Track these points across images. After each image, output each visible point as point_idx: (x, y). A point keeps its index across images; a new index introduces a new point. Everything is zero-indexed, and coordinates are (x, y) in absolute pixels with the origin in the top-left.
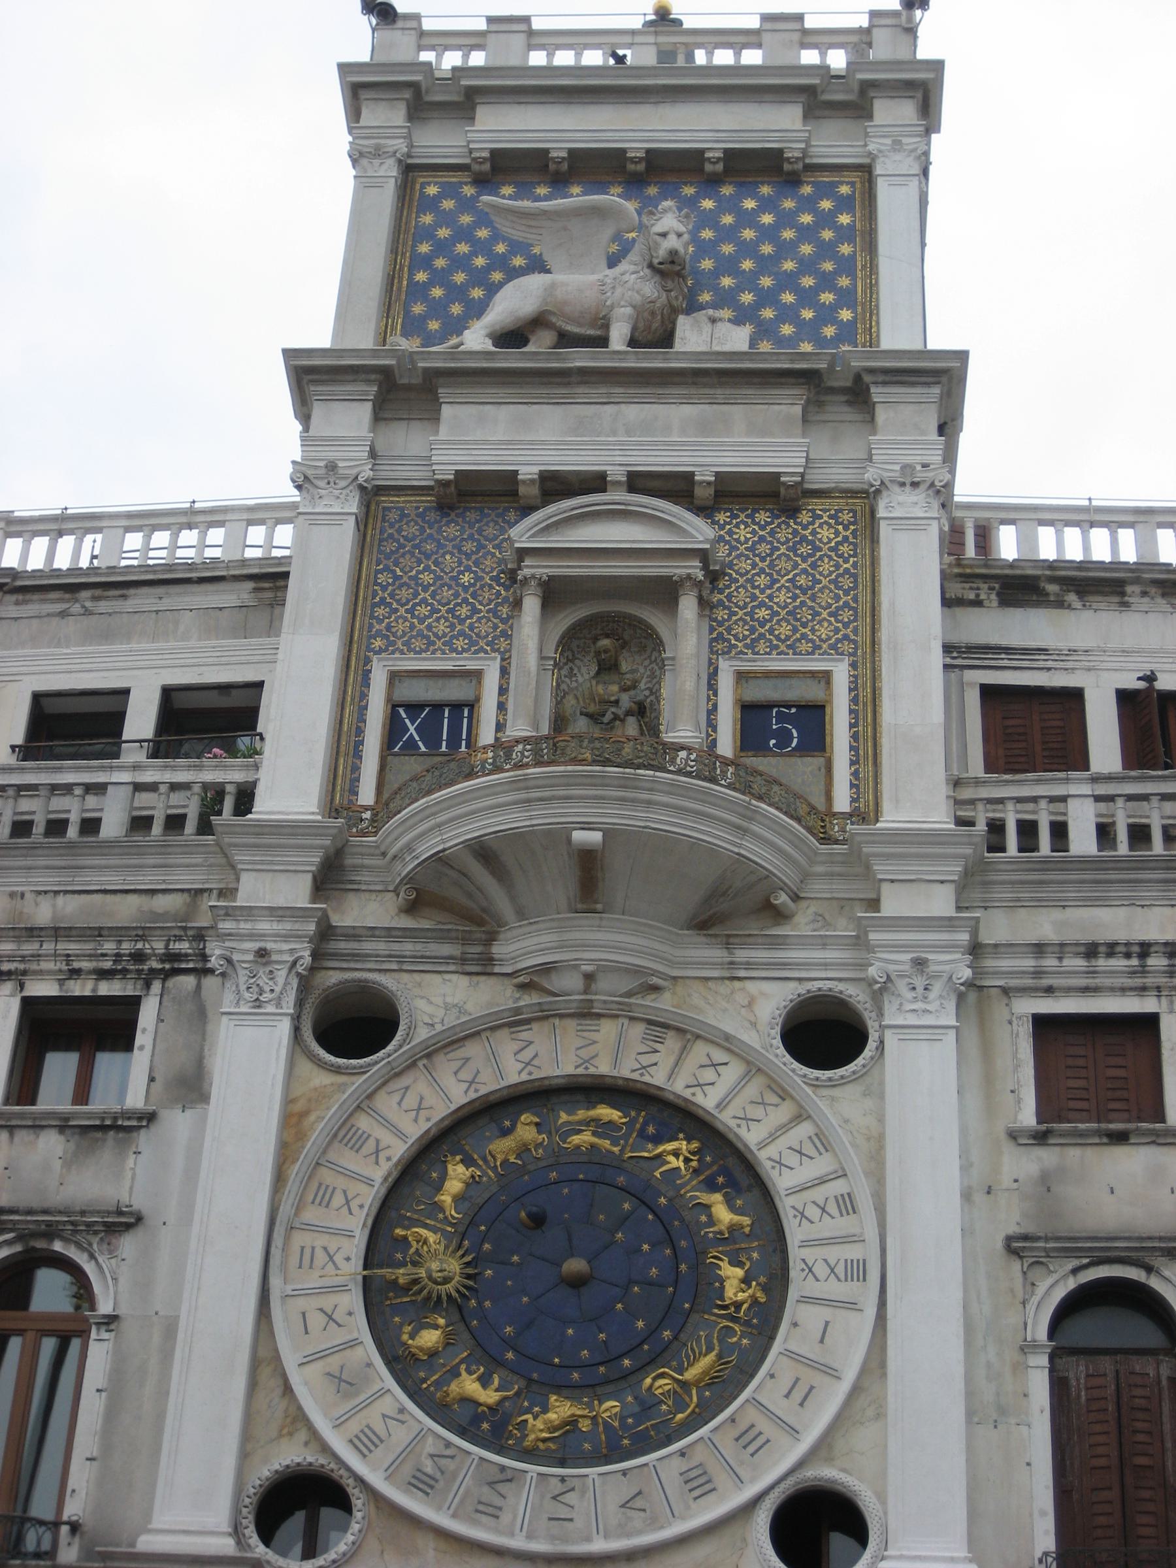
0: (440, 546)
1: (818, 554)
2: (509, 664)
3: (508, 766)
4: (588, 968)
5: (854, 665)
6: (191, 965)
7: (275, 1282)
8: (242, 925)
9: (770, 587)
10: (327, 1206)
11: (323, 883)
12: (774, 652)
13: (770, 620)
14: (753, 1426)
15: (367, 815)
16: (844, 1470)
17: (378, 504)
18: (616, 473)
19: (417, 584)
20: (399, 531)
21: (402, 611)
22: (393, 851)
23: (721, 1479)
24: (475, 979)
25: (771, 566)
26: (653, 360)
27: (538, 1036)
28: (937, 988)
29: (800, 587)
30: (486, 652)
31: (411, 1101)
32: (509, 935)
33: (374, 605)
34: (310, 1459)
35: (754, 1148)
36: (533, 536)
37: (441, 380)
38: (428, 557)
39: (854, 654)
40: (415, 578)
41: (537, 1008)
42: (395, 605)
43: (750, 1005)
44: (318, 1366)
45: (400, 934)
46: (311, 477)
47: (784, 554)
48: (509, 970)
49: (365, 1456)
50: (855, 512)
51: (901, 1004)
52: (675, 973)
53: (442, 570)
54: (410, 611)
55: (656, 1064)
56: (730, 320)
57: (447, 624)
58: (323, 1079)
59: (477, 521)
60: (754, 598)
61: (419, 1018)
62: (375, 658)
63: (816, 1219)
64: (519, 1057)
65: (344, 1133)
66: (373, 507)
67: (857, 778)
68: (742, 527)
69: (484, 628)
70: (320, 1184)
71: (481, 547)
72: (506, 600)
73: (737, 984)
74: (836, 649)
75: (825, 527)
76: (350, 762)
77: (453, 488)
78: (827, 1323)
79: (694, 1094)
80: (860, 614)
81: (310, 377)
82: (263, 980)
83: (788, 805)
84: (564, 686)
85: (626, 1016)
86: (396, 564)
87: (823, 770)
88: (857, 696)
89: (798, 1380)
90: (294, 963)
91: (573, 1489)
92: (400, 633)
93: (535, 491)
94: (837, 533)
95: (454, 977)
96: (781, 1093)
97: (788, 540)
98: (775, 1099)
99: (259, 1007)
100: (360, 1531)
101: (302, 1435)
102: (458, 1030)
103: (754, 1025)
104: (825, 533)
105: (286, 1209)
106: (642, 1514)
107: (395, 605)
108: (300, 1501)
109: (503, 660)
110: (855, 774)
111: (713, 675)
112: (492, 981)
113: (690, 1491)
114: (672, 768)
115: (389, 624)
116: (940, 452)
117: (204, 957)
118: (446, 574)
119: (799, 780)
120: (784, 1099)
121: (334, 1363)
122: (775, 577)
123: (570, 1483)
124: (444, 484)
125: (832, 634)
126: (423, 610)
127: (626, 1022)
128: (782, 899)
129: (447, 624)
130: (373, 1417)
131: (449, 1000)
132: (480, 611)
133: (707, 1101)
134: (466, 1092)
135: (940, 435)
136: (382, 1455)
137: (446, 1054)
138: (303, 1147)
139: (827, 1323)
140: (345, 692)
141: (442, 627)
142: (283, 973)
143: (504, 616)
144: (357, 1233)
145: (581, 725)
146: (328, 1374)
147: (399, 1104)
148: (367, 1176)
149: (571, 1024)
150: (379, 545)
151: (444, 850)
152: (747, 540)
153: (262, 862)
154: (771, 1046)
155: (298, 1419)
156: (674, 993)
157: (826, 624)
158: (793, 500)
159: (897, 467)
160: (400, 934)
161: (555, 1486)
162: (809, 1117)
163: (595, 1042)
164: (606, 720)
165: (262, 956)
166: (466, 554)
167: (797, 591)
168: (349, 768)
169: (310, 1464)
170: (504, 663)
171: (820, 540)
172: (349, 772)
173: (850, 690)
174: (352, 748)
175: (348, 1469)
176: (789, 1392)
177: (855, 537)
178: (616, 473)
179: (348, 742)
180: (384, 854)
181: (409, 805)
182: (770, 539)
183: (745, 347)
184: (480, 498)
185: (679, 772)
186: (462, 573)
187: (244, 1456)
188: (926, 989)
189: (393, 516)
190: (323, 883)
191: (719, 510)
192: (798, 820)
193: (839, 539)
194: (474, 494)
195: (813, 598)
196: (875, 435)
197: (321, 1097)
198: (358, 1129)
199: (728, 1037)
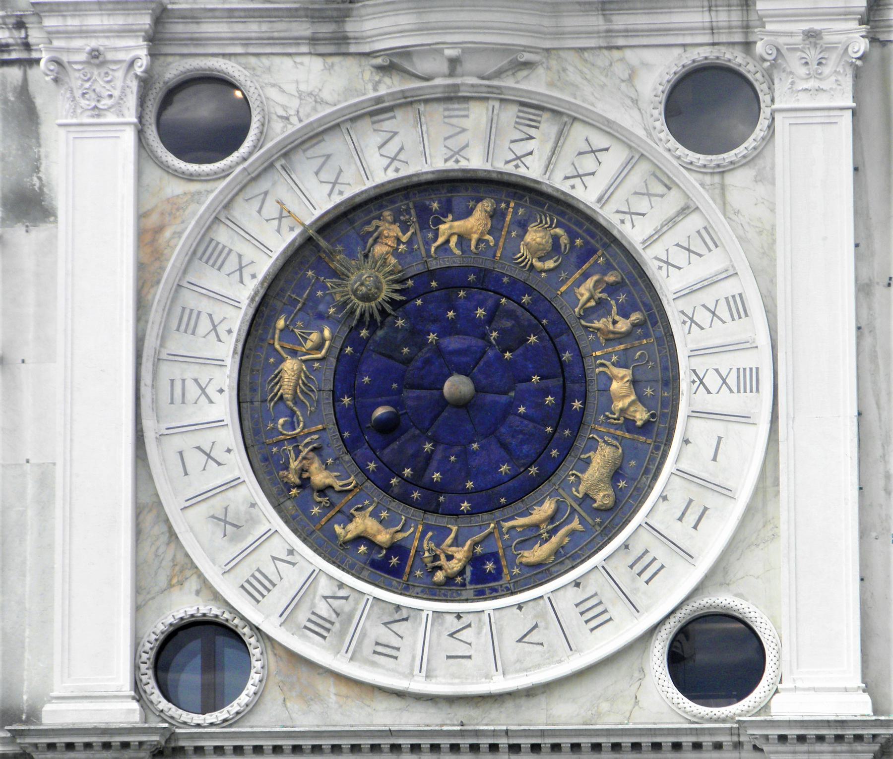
4: (450, 52)
6: (14, 56)
7: (149, 424)
10: (193, 333)
14: (647, 552)
16: (739, 595)
23: (618, 610)
24: (330, 60)
27: (401, 124)
28: (833, 58)
31: (270, 208)
32: (363, 11)
34: (203, 610)
35: (639, 248)
41: (400, 96)
43: (630, 80)
44: (202, 510)
45: (242, 14)
48: (367, 49)
49: (258, 602)
51: (793, 83)
52: (548, 44)
55: (531, 153)
58: (176, 188)
61: (272, 110)
63: (706, 325)
64: (384, 151)
65: (205, 250)
70: (184, 309)
73: (616, 54)
78: (720, 439)
79: (573, 187)
82: (100, 85)
85: (496, 99)
89: (691, 501)
90: (132, 64)
91: (469, 626)
95: (306, 60)
96: (667, 182)
98: (661, 189)
99: (98, 116)
100: (260, 681)
101: (193, 584)
102: (315, 125)
103: (635, 102)
105: (151, 342)
106: (539, 648)
108: (195, 652)
112: (349, 62)
113: (587, 622)
117: (27, 46)
120: (669, 189)
121: (216, 504)
123: (465, 620)
127: (497, 104)
130: (262, 560)
131: (303, 87)
133: (586, 195)
134: (330, 195)
136: (278, 599)
137: (304, 151)
138: (163, 269)
139: (720, 439)
142: (120, 74)
144: (229, 361)
146: (213, 517)
147: (259, 212)
148: (230, 298)
149: (438, 110)
154: (655, 128)
155: (186, 568)
156: (548, 68)
160: (242, 14)
161: (451, 623)
162: (697, 208)
163: (464, 130)
165: (97, 57)
169: (204, 615)
175: (243, 618)
176: (683, 514)
187: (138, 609)
188: (820, 64)
197: (175, 207)
198: (218, 243)
199: (609, 121)
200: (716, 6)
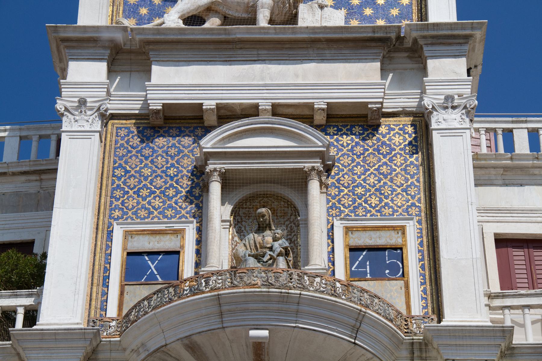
1: (393, 153)
3: (207, 290)
12: (369, 215)
15: (114, 323)
18: (265, 105)
19: (140, 176)
20: (128, 142)
22: (134, 346)
26: (285, 33)
29: (382, 174)
30: (186, 218)
36: (215, 144)
37: (151, 47)
38: (146, 158)
39: (419, 215)
40: (139, 172)
42: (126, 189)
46: (69, 108)
47: (371, 153)
53: (156, 167)
54: (137, 193)
56: (331, 6)
57: (161, 200)
60: (354, 181)
62: (115, 224)
74: (408, 212)
75: (397, 136)
76: (100, 290)
81: (66, 44)
83: (385, 311)
86: (126, 162)
87: (403, 288)
92: (130, 207)
104: (397, 139)
107: (126, 189)
114: (311, 289)
115: (123, 201)
116: (470, 87)
119: (389, 295)
122: (367, 167)
124: (157, 112)
125: (404, 203)
126: (145, 192)
129: (161, 200)
135: (468, 76)
140: (96, 245)
143: (197, 195)
145: (252, 262)
150: (115, 152)
151: (166, 345)
152: (348, 145)
157: (400, 196)
158: (376, 119)
159: (443, 97)
164: (265, 259)
167: (381, 176)
168: (100, 294)
171: (394, 144)
172: (100, 296)
173: (418, 237)
174: (101, 281)
177: (416, 142)
178: (265, 105)
180: (124, 350)
181: (142, 316)
183: (342, 23)
184: (178, 121)
185: (316, 291)
186: (168, 168)
191: (330, 126)
192: (391, 321)
194: (175, 118)
195: (391, 180)
196: (426, 77)
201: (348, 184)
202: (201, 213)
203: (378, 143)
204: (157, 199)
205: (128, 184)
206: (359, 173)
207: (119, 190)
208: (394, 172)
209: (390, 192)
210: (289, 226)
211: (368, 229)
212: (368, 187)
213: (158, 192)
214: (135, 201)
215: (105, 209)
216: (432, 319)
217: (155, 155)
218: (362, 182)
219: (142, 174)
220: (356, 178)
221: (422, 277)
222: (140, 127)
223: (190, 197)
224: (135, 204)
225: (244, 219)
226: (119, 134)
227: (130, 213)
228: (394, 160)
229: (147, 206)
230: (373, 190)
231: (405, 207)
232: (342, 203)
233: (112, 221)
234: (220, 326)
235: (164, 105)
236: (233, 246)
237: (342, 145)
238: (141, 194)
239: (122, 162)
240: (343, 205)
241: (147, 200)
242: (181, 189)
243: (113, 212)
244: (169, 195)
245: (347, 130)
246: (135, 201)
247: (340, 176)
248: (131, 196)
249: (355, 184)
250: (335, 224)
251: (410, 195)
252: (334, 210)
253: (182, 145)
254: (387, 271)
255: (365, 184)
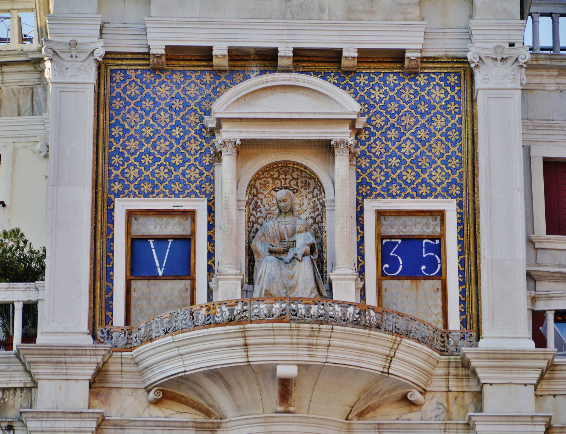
0: (155, 104)
1: (433, 111)
2: (213, 204)
5: (460, 205)
8: (44, 424)
9: (398, 140)
11: (94, 382)
13: (399, 168)
17: (107, 66)
19: (141, 136)
20: (124, 90)
21: (132, 159)
25: (399, 121)
29: (420, 140)
32: (229, 425)
33: (111, 155)
38: (147, 114)
39: (460, 195)
40: (139, 132)
45: (152, 424)
50: (459, 75)
53: (159, 125)
59: (183, 83)
60: (387, 148)
62: (116, 200)
66: (103, 70)
67: (464, 296)
68: (377, 88)
69: (193, 174)
71: (186, 105)
72: (208, 150)
75: (438, 88)
76: (104, 285)
77: (164, 59)
80: (464, 162)
84: (252, 218)
88: (462, 229)
92: (132, 178)
93: (224, 63)
94: (446, 94)
97: (411, 100)
104: (438, 94)
109: (209, 201)
110: (463, 293)
111: (360, 213)
118: (162, 127)
128: (416, 396)
129: (166, 171)
132: (189, 160)
141: (162, 173)
143: (207, 164)
151: (185, 371)
153: (53, 374)
157: (439, 170)
160: (152, 424)
166: (175, 111)
168: (104, 290)
170: (210, 204)
171: (434, 99)
172: (104, 293)
174: (104, 273)
179: (102, 269)
182: (397, 99)
184: (182, 63)
186: (173, 127)
189: (118, 77)
190: (94, 382)
193: (448, 98)
200: (449, 429)
201: (381, 153)
202: (213, 188)
203: (415, 97)
204: (162, 168)
205: (128, 148)
206: (393, 139)
207: (117, 156)
208: (433, 138)
209: (427, 165)
210: (313, 200)
211: (403, 213)
212: (403, 158)
213: (163, 159)
214: (137, 171)
215: (103, 180)
216: (471, 335)
217: (157, 108)
218: (397, 151)
219: (144, 134)
220: (390, 145)
221: (461, 276)
222: (136, 70)
223: (199, 167)
224: (137, 176)
225: (260, 191)
226: (114, 79)
227: (132, 186)
228: (434, 121)
229: (151, 178)
230: (409, 161)
231: (445, 184)
232: (374, 178)
233: (112, 196)
234: (245, 360)
235: (168, 48)
236: (250, 230)
237: (374, 100)
238: (143, 161)
239: (119, 118)
240: (375, 181)
241: (151, 170)
242: (188, 157)
243: (112, 185)
244: (175, 163)
245: (380, 79)
246: (137, 171)
247: (371, 142)
248: (131, 164)
249: (389, 153)
250: (365, 207)
251: (450, 168)
252: (364, 189)
253: (187, 96)
254: (423, 267)
255: (399, 153)
